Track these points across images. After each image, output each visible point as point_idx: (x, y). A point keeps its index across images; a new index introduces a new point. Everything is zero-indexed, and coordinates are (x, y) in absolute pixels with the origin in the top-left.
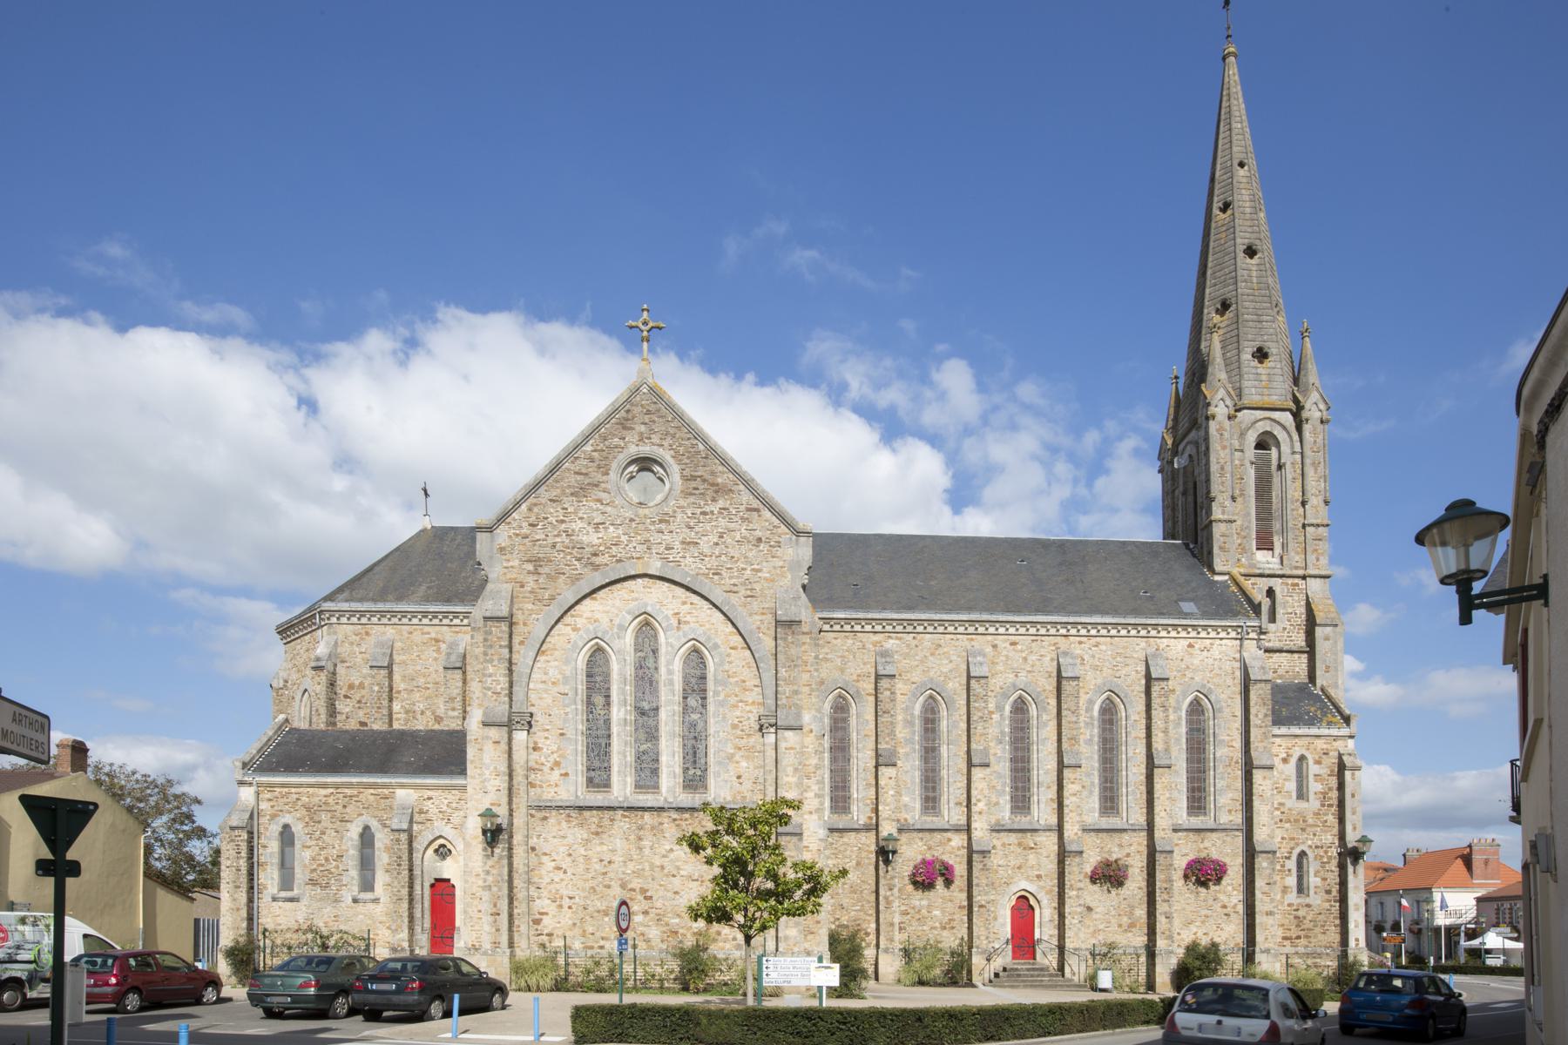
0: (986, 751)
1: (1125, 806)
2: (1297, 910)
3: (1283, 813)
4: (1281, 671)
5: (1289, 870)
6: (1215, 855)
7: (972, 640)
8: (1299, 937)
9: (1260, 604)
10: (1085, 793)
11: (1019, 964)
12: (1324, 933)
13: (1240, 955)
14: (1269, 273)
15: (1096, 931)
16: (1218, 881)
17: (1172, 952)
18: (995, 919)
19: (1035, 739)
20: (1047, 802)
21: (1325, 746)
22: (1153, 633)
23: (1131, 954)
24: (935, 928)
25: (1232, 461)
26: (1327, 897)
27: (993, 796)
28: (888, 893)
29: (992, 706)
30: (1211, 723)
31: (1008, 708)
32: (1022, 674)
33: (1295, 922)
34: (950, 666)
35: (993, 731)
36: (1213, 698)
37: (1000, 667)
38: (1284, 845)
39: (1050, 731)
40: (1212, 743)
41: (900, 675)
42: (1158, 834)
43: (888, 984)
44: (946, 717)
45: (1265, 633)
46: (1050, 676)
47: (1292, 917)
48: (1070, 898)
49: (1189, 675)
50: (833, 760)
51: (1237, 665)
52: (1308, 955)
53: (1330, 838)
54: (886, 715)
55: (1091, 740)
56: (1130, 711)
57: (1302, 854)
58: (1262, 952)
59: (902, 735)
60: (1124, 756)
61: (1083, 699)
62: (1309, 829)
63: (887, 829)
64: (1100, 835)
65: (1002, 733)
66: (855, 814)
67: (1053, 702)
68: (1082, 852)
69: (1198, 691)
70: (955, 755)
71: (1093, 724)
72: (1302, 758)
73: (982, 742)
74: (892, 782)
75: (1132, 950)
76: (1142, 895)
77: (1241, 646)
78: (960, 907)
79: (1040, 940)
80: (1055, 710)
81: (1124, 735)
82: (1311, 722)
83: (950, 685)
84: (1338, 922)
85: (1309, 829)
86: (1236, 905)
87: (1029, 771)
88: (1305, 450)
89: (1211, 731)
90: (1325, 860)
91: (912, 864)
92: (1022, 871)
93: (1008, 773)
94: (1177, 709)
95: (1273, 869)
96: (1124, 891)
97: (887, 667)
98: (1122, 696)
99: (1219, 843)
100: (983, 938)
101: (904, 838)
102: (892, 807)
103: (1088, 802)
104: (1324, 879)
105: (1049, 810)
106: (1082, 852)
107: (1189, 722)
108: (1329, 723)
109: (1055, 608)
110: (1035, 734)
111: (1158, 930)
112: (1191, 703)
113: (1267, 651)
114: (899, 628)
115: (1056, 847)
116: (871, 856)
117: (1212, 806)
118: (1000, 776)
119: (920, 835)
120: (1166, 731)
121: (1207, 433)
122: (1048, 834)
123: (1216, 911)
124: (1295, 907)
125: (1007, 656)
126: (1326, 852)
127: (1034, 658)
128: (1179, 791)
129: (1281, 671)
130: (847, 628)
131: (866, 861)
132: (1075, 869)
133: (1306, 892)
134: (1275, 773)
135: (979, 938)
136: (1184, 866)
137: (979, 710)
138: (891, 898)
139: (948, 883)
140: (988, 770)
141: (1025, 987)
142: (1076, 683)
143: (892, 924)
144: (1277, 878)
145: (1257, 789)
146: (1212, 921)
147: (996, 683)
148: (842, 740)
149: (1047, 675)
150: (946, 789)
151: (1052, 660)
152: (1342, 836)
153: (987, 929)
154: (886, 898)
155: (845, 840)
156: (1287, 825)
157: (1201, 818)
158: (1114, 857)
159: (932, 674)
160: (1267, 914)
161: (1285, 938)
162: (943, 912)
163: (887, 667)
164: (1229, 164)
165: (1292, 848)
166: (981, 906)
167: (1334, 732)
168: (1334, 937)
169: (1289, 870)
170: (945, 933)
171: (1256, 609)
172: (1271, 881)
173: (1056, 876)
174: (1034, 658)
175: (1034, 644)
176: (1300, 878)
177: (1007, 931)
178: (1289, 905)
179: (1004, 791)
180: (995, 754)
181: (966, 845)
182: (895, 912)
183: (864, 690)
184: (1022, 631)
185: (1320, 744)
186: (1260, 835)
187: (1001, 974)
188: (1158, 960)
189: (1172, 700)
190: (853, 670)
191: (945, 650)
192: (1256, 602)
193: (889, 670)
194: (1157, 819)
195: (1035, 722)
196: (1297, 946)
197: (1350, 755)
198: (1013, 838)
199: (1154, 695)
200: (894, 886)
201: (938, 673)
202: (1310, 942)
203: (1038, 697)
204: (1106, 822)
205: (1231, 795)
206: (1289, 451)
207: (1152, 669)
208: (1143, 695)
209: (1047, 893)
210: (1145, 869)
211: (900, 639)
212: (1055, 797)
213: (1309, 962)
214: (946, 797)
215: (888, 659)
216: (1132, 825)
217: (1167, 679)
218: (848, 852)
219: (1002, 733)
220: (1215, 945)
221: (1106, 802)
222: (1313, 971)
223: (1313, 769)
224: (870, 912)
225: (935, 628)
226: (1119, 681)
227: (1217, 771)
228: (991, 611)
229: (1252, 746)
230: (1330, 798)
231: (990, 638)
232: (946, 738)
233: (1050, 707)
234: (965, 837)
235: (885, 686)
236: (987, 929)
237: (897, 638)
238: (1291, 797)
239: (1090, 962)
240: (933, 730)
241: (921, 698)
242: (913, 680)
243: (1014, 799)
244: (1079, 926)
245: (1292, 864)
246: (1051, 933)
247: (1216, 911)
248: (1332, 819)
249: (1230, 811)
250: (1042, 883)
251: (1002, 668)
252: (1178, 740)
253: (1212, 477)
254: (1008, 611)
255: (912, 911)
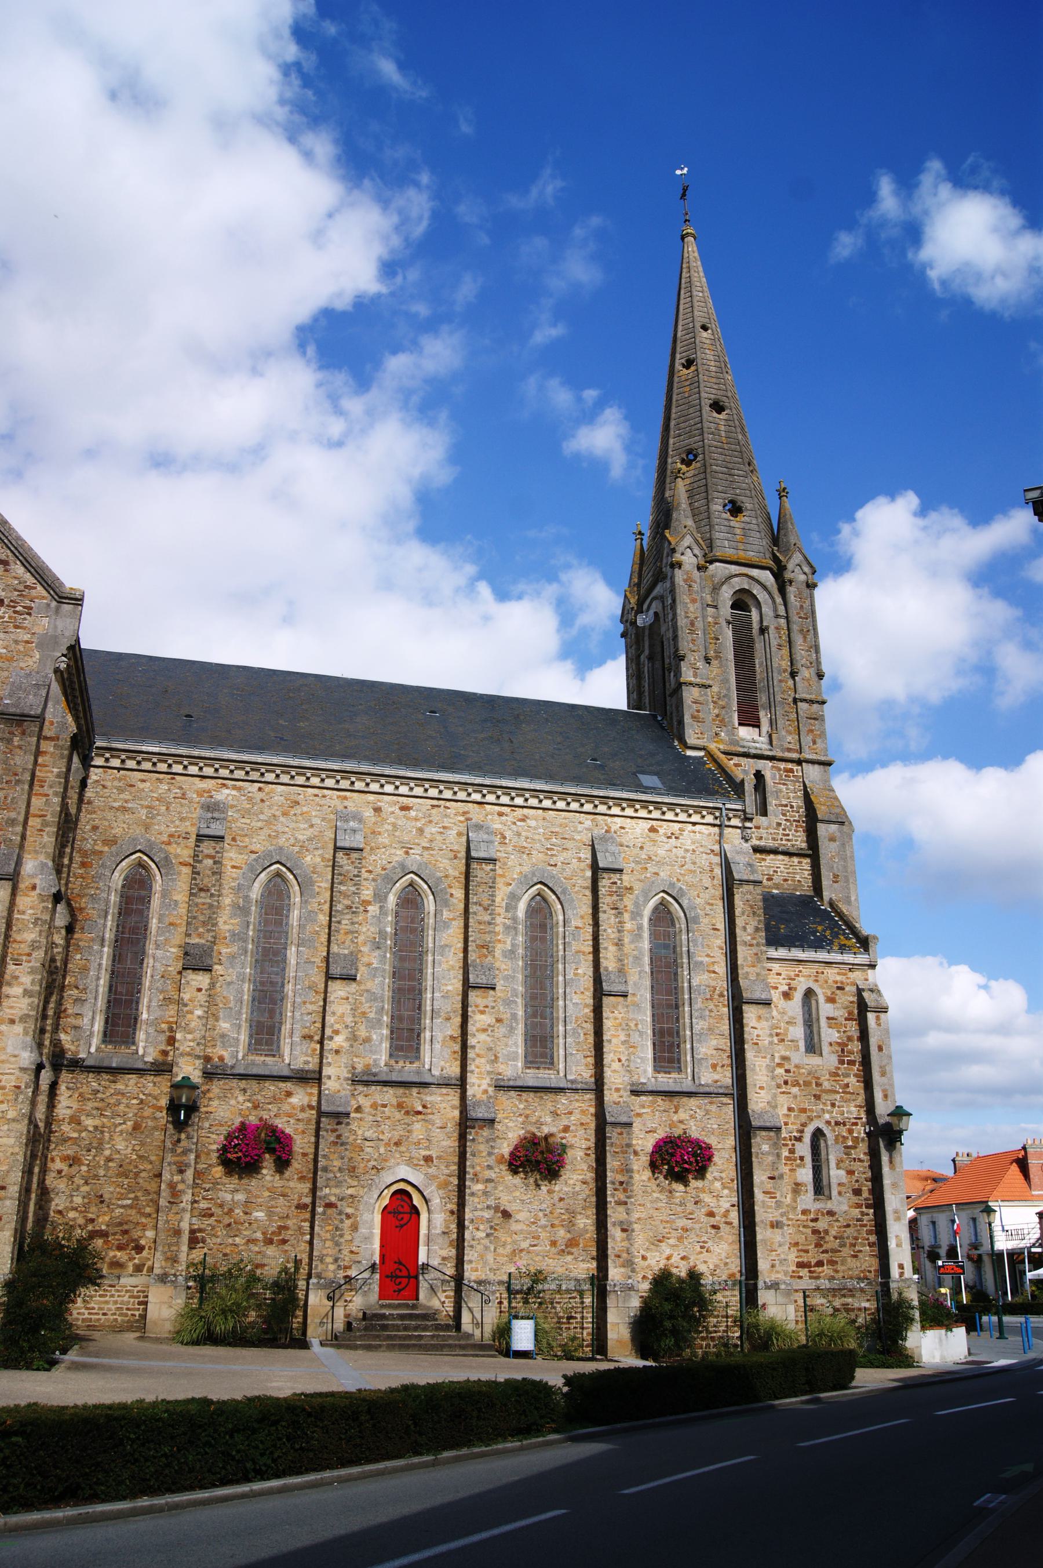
0: (353, 958)
1: (562, 1052)
2: (815, 1220)
3: (787, 1071)
4: (777, 879)
5: (802, 1158)
6: (695, 1133)
7: (345, 798)
8: (820, 1264)
9: (743, 781)
10: (501, 1030)
11: (389, 1306)
12: (855, 1256)
13: (737, 1293)
14: (739, 430)
15: (516, 1252)
16: (701, 1173)
17: (631, 1288)
18: (355, 1228)
19: (431, 945)
20: (444, 1041)
21: (839, 978)
22: (602, 809)
23: (568, 1291)
24: (254, 1241)
25: (704, 617)
26: (855, 1199)
27: (363, 1028)
28: (177, 1178)
29: (367, 893)
30: (684, 937)
31: (392, 900)
32: (417, 850)
33: (813, 1238)
34: (309, 833)
35: (367, 931)
36: (685, 903)
37: (383, 839)
38: (792, 1120)
39: (453, 935)
40: (685, 966)
41: (234, 839)
42: (609, 1097)
43: (158, 1340)
44: (298, 905)
45: (751, 820)
46: (456, 857)
47: (809, 1231)
48: (473, 1194)
49: (652, 868)
50: (117, 958)
51: (717, 859)
52: (834, 1292)
53: (853, 1110)
54: (203, 894)
55: (512, 952)
56: (569, 913)
57: (818, 1134)
58: (768, 1287)
59: (227, 927)
60: (561, 978)
61: (502, 894)
62: (824, 1096)
63: (189, 1069)
64: (525, 1095)
65: (382, 933)
66: (141, 1044)
67: (459, 893)
68: (492, 1121)
69: (664, 891)
70: (308, 962)
71: (515, 928)
72: (809, 993)
73: (347, 943)
74: (202, 997)
75: (572, 1285)
76: (587, 1193)
77: (721, 835)
78: (298, 1207)
79: (426, 1266)
80: (462, 906)
81: (561, 947)
82: (818, 944)
83: (308, 858)
84: (873, 1238)
85: (824, 1096)
86: (728, 1211)
87: (420, 994)
88: (790, 615)
89: (685, 949)
90: (850, 1143)
91: (224, 1131)
92: (402, 1149)
93: (387, 994)
94: (636, 915)
95: (778, 1156)
96: (558, 1186)
97: (213, 826)
98: (558, 891)
99: (700, 1113)
100: (329, 1260)
101: (216, 1088)
102: (198, 1035)
103: (506, 1045)
104: (850, 1173)
105: (447, 1053)
106: (492, 1121)
107: (654, 935)
108: (843, 949)
109: (467, 766)
110: (430, 939)
111: (609, 1252)
112: (656, 909)
113: (757, 850)
114: (239, 774)
115: (457, 1113)
116: (159, 1114)
117: (689, 1058)
118: (374, 998)
119: (243, 1084)
120: (619, 944)
121: (673, 583)
122: (444, 1091)
123: (698, 1222)
124: (812, 1216)
125: (394, 825)
126: (850, 1131)
127: (434, 830)
128: (641, 1034)
129: (777, 879)
130: (162, 767)
131: (150, 1123)
132: (482, 1147)
133: (826, 1193)
134: (775, 1013)
135: (322, 1261)
136: (649, 1148)
137: (346, 896)
138: (180, 1187)
139: (282, 1165)
140: (354, 985)
141: (391, 1348)
142: (491, 867)
143: (178, 1233)
144: (785, 1170)
145: (749, 1034)
146: (693, 1237)
147: (378, 860)
148: (134, 930)
149: (451, 855)
150: (289, 1014)
151: (459, 834)
152: (870, 1106)
153: (337, 1244)
154: (172, 1186)
155: (120, 1086)
156: (795, 1090)
157: (674, 1075)
158: (546, 1130)
159: (282, 841)
160: (772, 1226)
161: (801, 1265)
162: (270, 1214)
163: (213, 826)
164: (691, 325)
165: (804, 1125)
166: (330, 1205)
167: (849, 958)
168: (869, 1262)
169: (802, 1158)
170: (271, 1251)
171: (738, 788)
172: (776, 1174)
173: (456, 1160)
174: (434, 830)
175: (434, 811)
176: (817, 1170)
177: (373, 1249)
178: (805, 1212)
179: (379, 1021)
180: (369, 965)
181: (314, 1104)
182: (184, 1210)
183: (177, 856)
184: (419, 791)
185: (832, 974)
186: (758, 1101)
187: (354, 1324)
188: (611, 1302)
189: (628, 901)
190: (163, 828)
191: (305, 809)
192: (738, 780)
193: (216, 829)
194: (608, 1073)
195: (432, 921)
196: (818, 1278)
197: (871, 990)
198: (389, 1095)
199: (602, 891)
200: (188, 1165)
201: (292, 841)
202: (837, 1271)
203: (437, 885)
204: (532, 1077)
205: (714, 1043)
206: (771, 614)
207: (599, 856)
208: (588, 893)
209: (439, 1187)
210: (591, 1152)
211: (239, 789)
212: (457, 1033)
213: (837, 1303)
214: (288, 1026)
215: (216, 815)
216: (572, 1082)
217: (621, 871)
218: (122, 1107)
219: (382, 933)
220: (694, 1276)
221: (534, 1046)
222: (842, 1319)
223: (826, 1010)
224: (148, 1210)
225: (292, 777)
226: (555, 871)
227: (695, 1007)
228: (375, 761)
229: (740, 971)
230: (851, 1052)
231: (371, 797)
232: (295, 936)
233: (455, 901)
234: (315, 1091)
235: (206, 851)
236: (337, 1244)
237: (234, 788)
238: (797, 1049)
239: (506, 1303)
240: (279, 923)
241: (263, 875)
242: (253, 848)
243: (395, 1033)
244: (486, 1242)
245: (804, 1149)
246: (444, 1253)
247: (698, 1222)
248: (854, 1082)
249: (714, 1066)
250: (432, 1170)
251: (387, 841)
252: (637, 959)
253: (680, 633)
254: (400, 762)
255: (218, 1211)
